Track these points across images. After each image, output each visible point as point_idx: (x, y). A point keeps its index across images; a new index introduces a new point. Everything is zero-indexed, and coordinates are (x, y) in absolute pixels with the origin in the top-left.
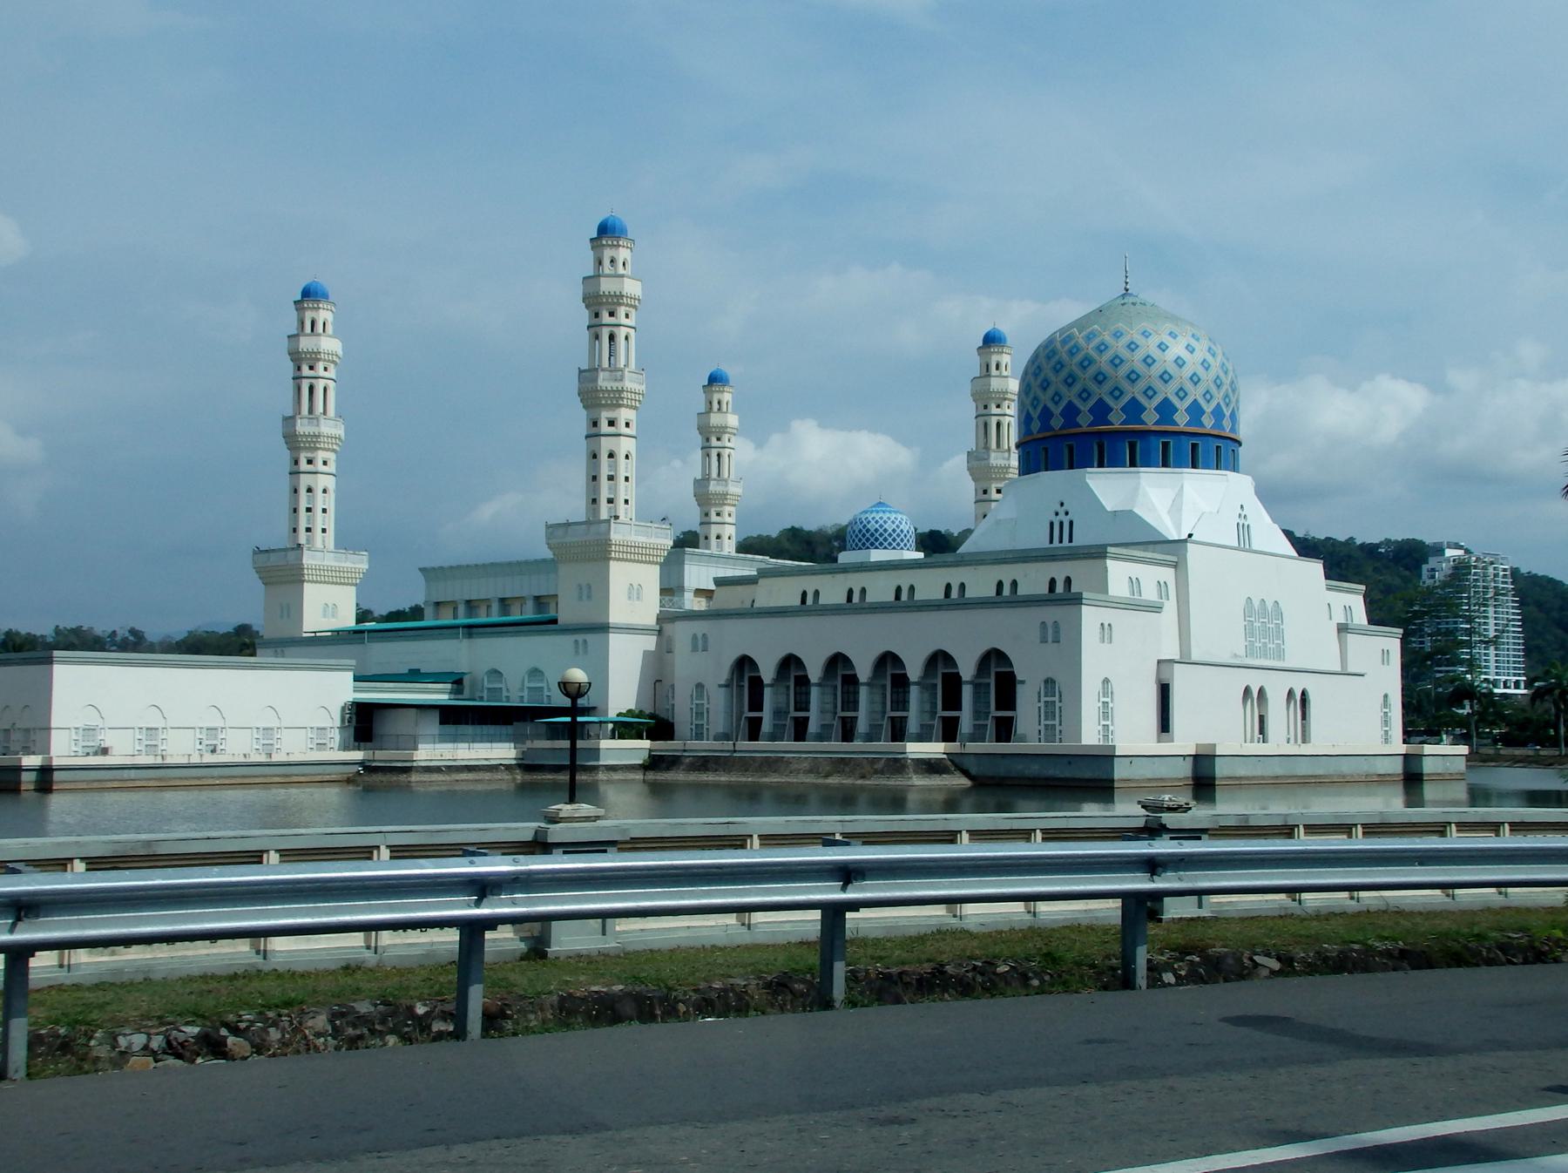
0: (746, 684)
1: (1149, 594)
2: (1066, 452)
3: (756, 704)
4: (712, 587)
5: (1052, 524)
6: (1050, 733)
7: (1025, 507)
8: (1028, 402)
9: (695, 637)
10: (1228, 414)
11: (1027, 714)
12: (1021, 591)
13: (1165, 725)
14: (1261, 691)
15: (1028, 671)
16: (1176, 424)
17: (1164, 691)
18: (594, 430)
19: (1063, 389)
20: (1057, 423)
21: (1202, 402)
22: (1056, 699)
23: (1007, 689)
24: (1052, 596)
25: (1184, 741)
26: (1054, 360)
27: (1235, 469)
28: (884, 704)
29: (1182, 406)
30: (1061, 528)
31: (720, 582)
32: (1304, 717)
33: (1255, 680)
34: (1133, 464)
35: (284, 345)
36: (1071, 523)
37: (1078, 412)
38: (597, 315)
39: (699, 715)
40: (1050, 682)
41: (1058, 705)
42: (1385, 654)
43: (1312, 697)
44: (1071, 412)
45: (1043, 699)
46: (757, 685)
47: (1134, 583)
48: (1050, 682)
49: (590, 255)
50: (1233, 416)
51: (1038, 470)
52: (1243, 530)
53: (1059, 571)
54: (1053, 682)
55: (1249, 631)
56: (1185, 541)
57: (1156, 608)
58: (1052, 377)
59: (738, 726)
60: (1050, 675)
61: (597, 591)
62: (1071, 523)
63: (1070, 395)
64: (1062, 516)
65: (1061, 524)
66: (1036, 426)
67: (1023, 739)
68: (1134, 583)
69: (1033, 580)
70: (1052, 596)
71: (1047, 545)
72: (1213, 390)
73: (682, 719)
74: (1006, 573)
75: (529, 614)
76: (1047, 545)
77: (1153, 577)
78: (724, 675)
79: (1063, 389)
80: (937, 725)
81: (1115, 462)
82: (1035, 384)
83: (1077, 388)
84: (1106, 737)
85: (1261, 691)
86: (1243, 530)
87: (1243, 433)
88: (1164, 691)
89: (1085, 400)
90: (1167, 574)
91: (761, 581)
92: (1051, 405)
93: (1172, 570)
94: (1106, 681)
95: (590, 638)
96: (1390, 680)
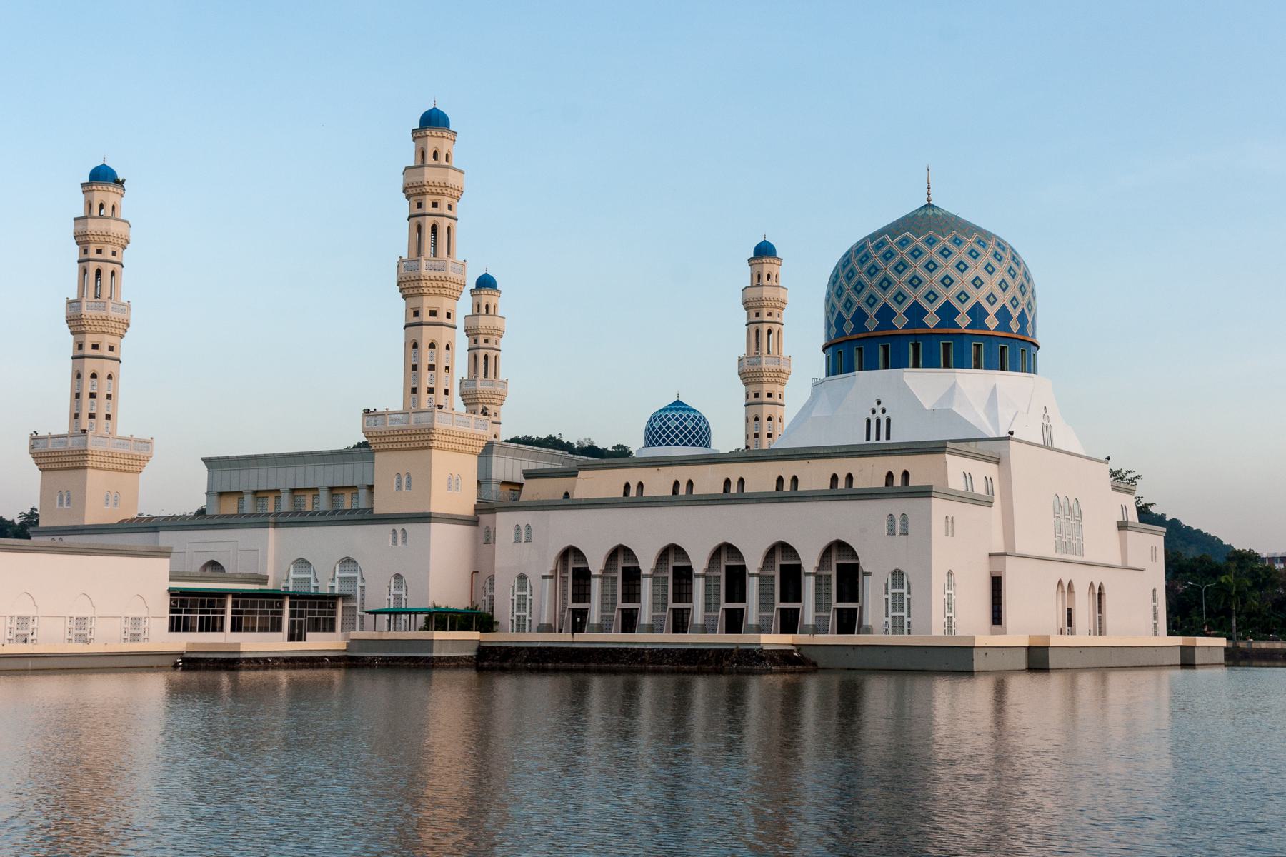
0: (570, 575)
1: (980, 489)
4: (523, 480)
5: (869, 421)
6: (898, 625)
8: (839, 305)
9: (518, 528)
10: (1030, 320)
11: (873, 603)
12: (857, 484)
14: (1070, 585)
15: (875, 563)
16: (959, 327)
17: (996, 583)
19: (878, 293)
20: (872, 324)
21: (1010, 307)
22: (905, 591)
24: (834, 492)
25: (1017, 633)
27: (1035, 372)
28: (615, 595)
29: (992, 310)
30: (878, 425)
31: (529, 475)
32: (1100, 612)
33: (1066, 573)
34: (947, 365)
35: (70, 228)
36: (889, 420)
38: (419, 205)
39: (521, 607)
40: (898, 575)
41: (906, 596)
42: (1154, 549)
43: (1106, 590)
44: (886, 314)
45: (890, 591)
46: (582, 576)
47: (968, 477)
48: (898, 575)
51: (851, 369)
52: (1047, 430)
53: (896, 465)
54: (902, 574)
55: (1058, 530)
56: (1008, 438)
57: (988, 503)
59: (562, 616)
60: (893, 569)
61: (418, 481)
62: (889, 420)
63: (886, 298)
64: (879, 413)
65: (878, 421)
66: (848, 328)
67: (868, 630)
68: (968, 477)
69: (870, 473)
71: (864, 442)
72: (1019, 296)
73: (504, 611)
74: (842, 467)
76: (864, 442)
77: (982, 470)
78: (549, 568)
79: (878, 293)
81: (931, 363)
83: (892, 291)
85: (1070, 585)
86: (1047, 430)
87: (1039, 339)
88: (996, 583)
89: (900, 303)
90: (991, 470)
91: (581, 474)
93: (995, 466)
94: (950, 573)
95: (410, 528)
96: (1157, 576)
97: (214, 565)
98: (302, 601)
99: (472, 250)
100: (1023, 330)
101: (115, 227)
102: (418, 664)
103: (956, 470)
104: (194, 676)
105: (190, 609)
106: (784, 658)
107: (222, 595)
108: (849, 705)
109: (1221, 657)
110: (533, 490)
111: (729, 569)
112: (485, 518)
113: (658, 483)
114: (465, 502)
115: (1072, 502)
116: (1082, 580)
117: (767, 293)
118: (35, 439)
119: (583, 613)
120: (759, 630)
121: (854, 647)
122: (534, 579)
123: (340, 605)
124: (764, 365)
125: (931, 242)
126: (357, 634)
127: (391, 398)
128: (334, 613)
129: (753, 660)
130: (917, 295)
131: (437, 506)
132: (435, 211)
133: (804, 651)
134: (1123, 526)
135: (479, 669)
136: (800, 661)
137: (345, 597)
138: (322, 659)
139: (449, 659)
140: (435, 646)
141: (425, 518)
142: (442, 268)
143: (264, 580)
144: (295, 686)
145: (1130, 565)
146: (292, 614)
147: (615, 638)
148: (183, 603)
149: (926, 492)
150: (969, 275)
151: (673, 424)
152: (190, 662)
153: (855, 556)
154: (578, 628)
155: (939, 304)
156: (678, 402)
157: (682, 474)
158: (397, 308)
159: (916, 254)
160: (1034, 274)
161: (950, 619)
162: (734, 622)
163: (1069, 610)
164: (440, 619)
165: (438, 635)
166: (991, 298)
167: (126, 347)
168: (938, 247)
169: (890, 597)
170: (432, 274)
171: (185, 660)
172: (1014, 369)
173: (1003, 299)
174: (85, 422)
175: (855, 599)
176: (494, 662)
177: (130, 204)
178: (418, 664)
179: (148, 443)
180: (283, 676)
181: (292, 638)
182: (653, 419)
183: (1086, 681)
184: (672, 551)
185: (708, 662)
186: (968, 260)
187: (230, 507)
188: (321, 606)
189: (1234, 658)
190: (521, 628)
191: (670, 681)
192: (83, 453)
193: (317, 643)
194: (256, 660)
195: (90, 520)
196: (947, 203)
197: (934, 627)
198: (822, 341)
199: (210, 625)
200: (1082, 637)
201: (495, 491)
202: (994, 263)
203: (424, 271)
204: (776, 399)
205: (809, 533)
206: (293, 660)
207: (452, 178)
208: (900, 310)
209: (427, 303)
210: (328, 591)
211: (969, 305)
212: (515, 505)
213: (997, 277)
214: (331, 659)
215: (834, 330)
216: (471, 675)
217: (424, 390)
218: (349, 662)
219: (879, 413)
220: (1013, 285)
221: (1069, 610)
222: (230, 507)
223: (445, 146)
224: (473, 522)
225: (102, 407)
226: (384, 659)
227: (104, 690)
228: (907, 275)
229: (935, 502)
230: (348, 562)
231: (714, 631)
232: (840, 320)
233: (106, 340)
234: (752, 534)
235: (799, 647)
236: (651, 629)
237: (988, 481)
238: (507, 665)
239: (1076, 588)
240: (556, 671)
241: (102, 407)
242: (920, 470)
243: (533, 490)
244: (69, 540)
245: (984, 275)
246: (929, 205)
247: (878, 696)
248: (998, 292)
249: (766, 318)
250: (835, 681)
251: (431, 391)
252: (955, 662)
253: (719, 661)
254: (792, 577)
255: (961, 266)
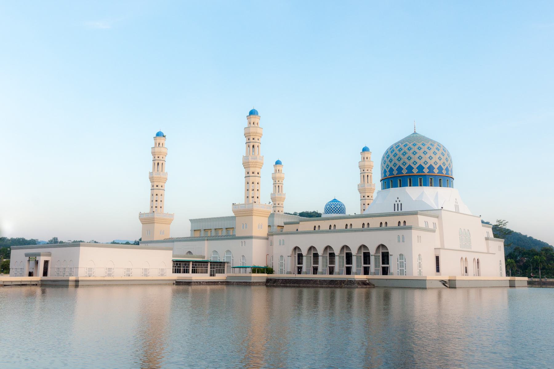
0: (297, 256)
1: (431, 226)
2: (399, 181)
3: (300, 262)
4: (283, 225)
6: (402, 272)
7: (384, 200)
8: (385, 166)
13: (438, 270)
14: (466, 259)
17: (437, 258)
18: (248, 175)
19: (397, 162)
20: (395, 173)
22: (404, 261)
23: (386, 257)
25: (445, 275)
26: (394, 153)
27: (453, 187)
29: (436, 167)
30: (398, 206)
31: (286, 224)
33: (464, 255)
34: (421, 185)
35: (150, 150)
37: (393, 170)
38: (249, 139)
39: (282, 266)
40: (401, 255)
42: (500, 247)
43: (480, 261)
44: (400, 169)
46: (300, 256)
47: (426, 223)
49: (246, 122)
50: (451, 170)
51: (389, 187)
52: (457, 207)
53: (402, 219)
58: (393, 158)
63: (400, 164)
66: (388, 174)
67: (392, 274)
68: (426, 223)
69: (393, 222)
70: (381, 228)
72: (446, 162)
73: (276, 268)
74: (383, 220)
75: (224, 233)
77: (431, 221)
80: (362, 270)
82: (387, 161)
83: (402, 161)
84: (420, 273)
85: (466, 259)
86: (457, 207)
88: (437, 258)
90: (435, 220)
92: (393, 167)
93: (436, 219)
94: (419, 255)
95: (247, 241)
97: (190, 252)
98: (213, 263)
99: (267, 153)
100: (447, 173)
101: (163, 150)
102: (247, 284)
103: (422, 220)
104: (181, 287)
105: (179, 266)
106: (364, 283)
107: (189, 262)
108: (387, 297)
109: (526, 284)
110: (287, 228)
111: (347, 254)
112: (270, 237)
113: (324, 225)
114: (264, 232)
115: (466, 231)
116: (471, 258)
117: (367, 163)
118: (141, 214)
119: (301, 268)
120: (356, 274)
121: (387, 279)
122: (285, 257)
123: (226, 265)
124: (366, 187)
125: (414, 145)
126: (231, 274)
127: (240, 199)
128: (224, 268)
129: (351, 283)
130: (410, 163)
131: (254, 234)
132: (253, 141)
133: (370, 281)
134: (487, 239)
135: (267, 286)
136: (368, 284)
137: (228, 263)
138: (218, 282)
139: (256, 283)
140: (252, 278)
141: (251, 237)
142: (256, 158)
143: (204, 257)
144: (212, 291)
145: (490, 252)
146: (211, 268)
147: (311, 276)
148: (177, 264)
149: (410, 228)
150: (428, 155)
151: (333, 206)
152: (178, 283)
153: (387, 249)
154: (299, 273)
155: (418, 165)
156: (335, 199)
157: (332, 223)
158: (243, 172)
159: (409, 149)
160: (452, 154)
161: (420, 270)
162: (349, 271)
163: (466, 267)
164: (255, 270)
165: (253, 275)
166: (436, 163)
167: (167, 186)
168: (417, 146)
169: (399, 263)
170: (253, 160)
171: (176, 282)
172: (445, 186)
173: (440, 163)
174: (154, 209)
175: (388, 264)
176: (271, 283)
177: (167, 142)
178: (247, 284)
179: (173, 215)
180: (208, 288)
181: (211, 275)
182: (327, 205)
183: (473, 292)
184: (328, 248)
185: (337, 284)
186: (427, 150)
187: (197, 234)
188: (220, 265)
189: (530, 284)
190: (282, 273)
191: (329, 290)
192: (153, 218)
193: (219, 277)
194: (197, 282)
195: (155, 239)
196: (421, 132)
197: (414, 273)
198: (380, 178)
199: (186, 271)
200: (471, 277)
201: (275, 229)
202: (436, 151)
203: (250, 160)
204: (370, 198)
205: (372, 242)
206: (209, 282)
207: (259, 131)
208: (404, 168)
209: (251, 170)
210: (222, 261)
211: (428, 165)
212: (281, 233)
213: (438, 156)
214: (221, 282)
215: (383, 175)
216: (265, 287)
217: (250, 197)
218: (227, 283)
219: (398, 202)
220: (443, 160)
221: (466, 267)
222: (197, 234)
223: (256, 121)
224: (267, 239)
225: (159, 204)
226: (237, 282)
227: (153, 291)
228: (407, 156)
229: (413, 231)
230: (228, 251)
231: (342, 274)
232: (385, 172)
233: (160, 184)
234: (354, 243)
235: (369, 279)
236: (322, 273)
237: (434, 224)
238: (275, 284)
239: (468, 260)
240: (290, 287)
241: (159, 204)
242: (410, 220)
243: (287, 228)
244: (150, 245)
245: (433, 155)
246: (415, 133)
247: (396, 295)
248: (438, 161)
249: (366, 171)
250: (382, 291)
251: (253, 197)
252: (420, 285)
253: (341, 284)
254: (367, 257)
255: (425, 153)
